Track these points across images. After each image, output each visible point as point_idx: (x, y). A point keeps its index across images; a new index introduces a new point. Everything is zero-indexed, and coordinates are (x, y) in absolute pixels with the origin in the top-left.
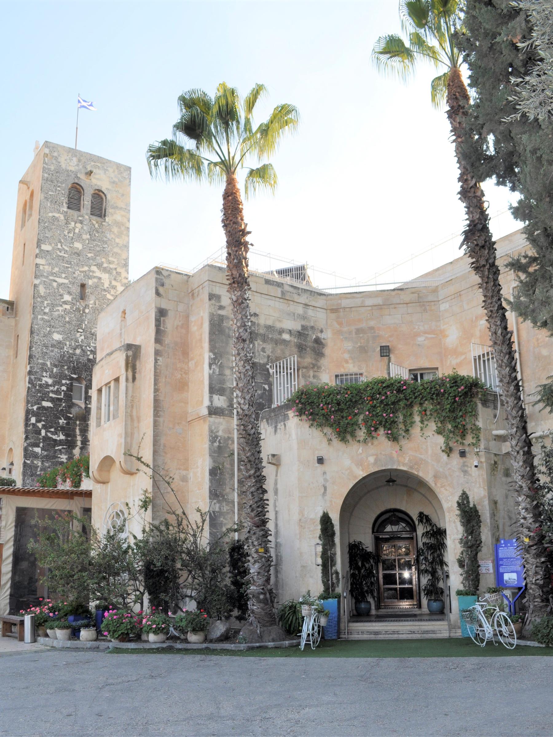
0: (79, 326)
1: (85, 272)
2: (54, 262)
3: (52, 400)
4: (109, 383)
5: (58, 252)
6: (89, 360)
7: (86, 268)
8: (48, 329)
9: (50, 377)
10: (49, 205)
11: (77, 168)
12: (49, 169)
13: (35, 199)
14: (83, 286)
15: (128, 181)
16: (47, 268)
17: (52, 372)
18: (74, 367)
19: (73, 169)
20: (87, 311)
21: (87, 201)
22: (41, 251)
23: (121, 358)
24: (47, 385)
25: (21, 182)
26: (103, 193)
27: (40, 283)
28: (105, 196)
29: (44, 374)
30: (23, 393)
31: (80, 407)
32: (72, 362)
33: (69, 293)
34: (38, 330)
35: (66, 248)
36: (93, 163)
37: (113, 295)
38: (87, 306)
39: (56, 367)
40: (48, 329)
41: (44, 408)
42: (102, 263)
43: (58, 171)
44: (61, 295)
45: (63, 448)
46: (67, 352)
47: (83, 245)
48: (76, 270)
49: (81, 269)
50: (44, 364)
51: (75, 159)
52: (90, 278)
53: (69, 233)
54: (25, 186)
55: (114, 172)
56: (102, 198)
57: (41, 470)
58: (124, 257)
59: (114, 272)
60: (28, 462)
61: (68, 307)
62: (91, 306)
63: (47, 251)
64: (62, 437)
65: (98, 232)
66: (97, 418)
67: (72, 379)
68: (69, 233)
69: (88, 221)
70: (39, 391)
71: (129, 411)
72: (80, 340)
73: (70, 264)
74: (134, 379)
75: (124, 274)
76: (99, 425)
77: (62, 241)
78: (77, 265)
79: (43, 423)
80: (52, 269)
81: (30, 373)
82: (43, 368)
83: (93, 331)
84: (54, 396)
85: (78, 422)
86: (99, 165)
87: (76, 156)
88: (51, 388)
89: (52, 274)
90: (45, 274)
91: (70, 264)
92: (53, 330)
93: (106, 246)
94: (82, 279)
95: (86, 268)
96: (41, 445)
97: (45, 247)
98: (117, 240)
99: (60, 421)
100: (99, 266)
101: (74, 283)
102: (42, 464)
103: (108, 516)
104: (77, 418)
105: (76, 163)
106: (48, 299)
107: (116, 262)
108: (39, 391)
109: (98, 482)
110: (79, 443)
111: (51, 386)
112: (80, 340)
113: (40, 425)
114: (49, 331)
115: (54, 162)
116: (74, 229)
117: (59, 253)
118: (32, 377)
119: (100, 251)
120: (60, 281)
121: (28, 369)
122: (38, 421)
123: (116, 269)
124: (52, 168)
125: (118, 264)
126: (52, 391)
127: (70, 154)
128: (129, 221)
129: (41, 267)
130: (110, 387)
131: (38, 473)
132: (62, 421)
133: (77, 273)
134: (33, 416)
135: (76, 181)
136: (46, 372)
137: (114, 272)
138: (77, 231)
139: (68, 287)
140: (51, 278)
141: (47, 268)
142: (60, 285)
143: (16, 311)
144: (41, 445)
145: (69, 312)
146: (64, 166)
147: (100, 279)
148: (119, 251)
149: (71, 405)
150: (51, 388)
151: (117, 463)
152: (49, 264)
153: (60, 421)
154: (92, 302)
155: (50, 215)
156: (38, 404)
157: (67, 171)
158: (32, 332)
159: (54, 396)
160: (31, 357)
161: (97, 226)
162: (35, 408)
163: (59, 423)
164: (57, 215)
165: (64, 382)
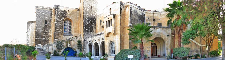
0: (91, 13)
14: (91, 6)
50: (86, 19)
64: (89, 30)
74: (115, 19)
81: (84, 20)
82: (86, 19)
100: (94, 3)
120: (87, 5)
121: (83, 19)
122: (86, 27)
132: (89, 28)
141: (86, 3)
145: (89, 10)
149: (90, 25)
160: (84, 17)
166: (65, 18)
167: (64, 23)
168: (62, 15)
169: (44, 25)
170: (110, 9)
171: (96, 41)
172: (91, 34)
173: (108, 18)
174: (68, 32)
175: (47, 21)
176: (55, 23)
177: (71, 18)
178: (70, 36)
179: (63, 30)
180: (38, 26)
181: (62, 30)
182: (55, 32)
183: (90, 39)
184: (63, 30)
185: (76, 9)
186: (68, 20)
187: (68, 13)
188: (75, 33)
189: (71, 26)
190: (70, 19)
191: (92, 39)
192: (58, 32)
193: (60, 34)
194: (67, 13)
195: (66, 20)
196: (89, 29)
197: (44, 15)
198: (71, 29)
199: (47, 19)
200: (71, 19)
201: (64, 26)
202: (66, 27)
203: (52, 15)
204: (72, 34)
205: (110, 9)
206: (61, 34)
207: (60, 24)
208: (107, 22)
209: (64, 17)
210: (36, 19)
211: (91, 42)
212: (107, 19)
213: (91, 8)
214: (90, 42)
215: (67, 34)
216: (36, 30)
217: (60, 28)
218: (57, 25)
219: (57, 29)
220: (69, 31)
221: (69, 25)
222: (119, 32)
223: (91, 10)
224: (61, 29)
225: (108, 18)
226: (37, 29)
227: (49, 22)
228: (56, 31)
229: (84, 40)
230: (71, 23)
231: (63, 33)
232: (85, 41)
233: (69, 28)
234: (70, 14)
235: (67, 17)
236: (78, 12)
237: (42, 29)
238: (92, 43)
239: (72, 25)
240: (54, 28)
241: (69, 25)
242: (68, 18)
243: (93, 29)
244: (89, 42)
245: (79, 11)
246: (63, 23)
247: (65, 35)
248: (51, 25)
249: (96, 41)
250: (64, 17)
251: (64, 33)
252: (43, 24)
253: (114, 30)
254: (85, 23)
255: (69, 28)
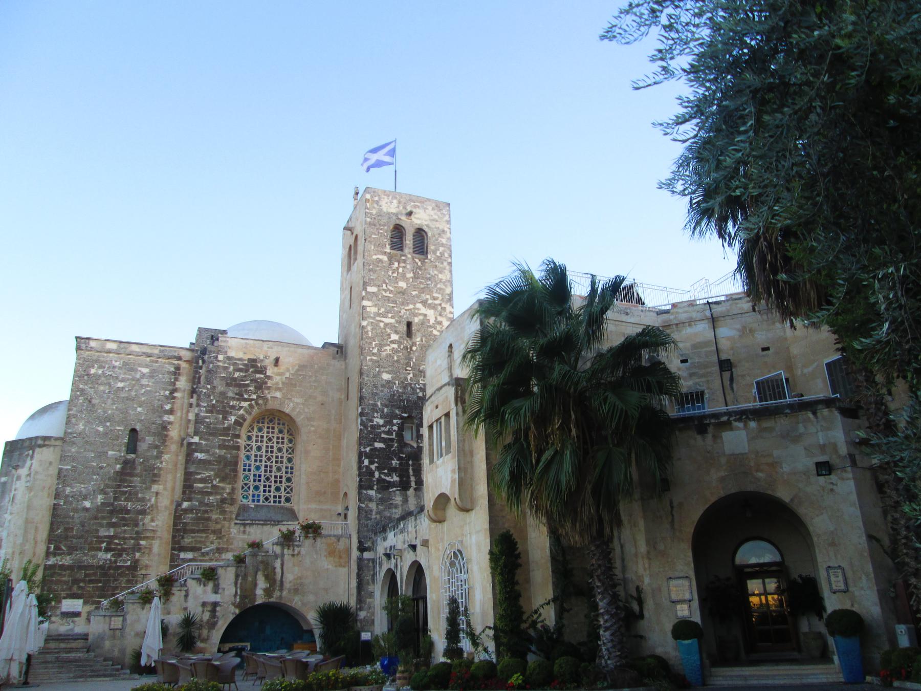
0: (408, 364)
1: (411, 309)
2: (380, 303)
3: (383, 441)
4: (440, 418)
5: (384, 293)
6: (419, 398)
7: (411, 306)
8: (377, 369)
9: (381, 418)
10: (373, 248)
11: (397, 209)
12: (371, 214)
13: (359, 242)
14: (409, 325)
15: (447, 216)
16: (374, 310)
17: (383, 412)
18: (404, 405)
19: (394, 211)
20: (414, 348)
21: (409, 241)
22: (367, 293)
23: (451, 392)
24: (379, 426)
25: (345, 228)
26: (424, 231)
27: (368, 325)
28: (426, 233)
29: (376, 415)
30: (356, 436)
31: (412, 447)
32: (402, 401)
33: (396, 332)
34: (367, 370)
35: (391, 288)
36: (412, 204)
37: (439, 331)
38: (414, 344)
39: (387, 407)
40: (377, 369)
41: (376, 449)
42: (427, 300)
43: (380, 214)
44: (389, 335)
45: (397, 490)
46: (398, 391)
47: (407, 284)
48: (401, 309)
49: (406, 308)
50: (375, 405)
51: (395, 201)
52: (416, 315)
53: (393, 273)
54: (349, 232)
55: (433, 209)
56: (423, 237)
57: (378, 513)
58: (448, 291)
59: (439, 308)
60: (363, 506)
61: (395, 346)
62: (418, 343)
63: (373, 293)
64: (396, 478)
65: (420, 269)
66: (430, 455)
67: (402, 418)
68: (393, 273)
69: (411, 260)
70: (371, 433)
71: (461, 446)
72: (409, 378)
73: (396, 303)
75: (449, 308)
76: (432, 461)
77: (387, 281)
78: (403, 304)
79: (376, 465)
80: (379, 310)
81: (361, 414)
82: (374, 409)
83: (421, 368)
84: (385, 436)
85: (411, 462)
86: (419, 204)
87: (396, 198)
88: (383, 429)
89: (379, 315)
90: (372, 315)
91: (396, 303)
92: (382, 370)
93: (429, 282)
94: (407, 318)
95: (411, 306)
96: (375, 487)
97: (371, 289)
98: (440, 276)
99: (393, 462)
100: (424, 303)
101: (400, 322)
102: (377, 507)
103: (446, 556)
104: (409, 457)
105: (396, 205)
106: (376, 340)
107: (440, 298)
108: (371, 433)
109: (435, 521)
110: (413, 484)
111: (382, 426)
112: (409, 378)
113: (373, 467)
114: (379, 371)
115: (376, 206)
116: (398, 269)
117: (384, 294)
118: (364, 418)
119: (424, 288)
120: (387, 320)
122: (371, 463)
123: (440, 305)
124: (374, 212)
125: (442, 300)
126: (384, 432)
127: (390, 198)
128: (450, 256)
129: (368, 309)
130: (440, 423)
131: (373, 517)
132: (395, 462)
133: (403, 311)
134: (366, 458)
135: (398, 222)
136: (377, 412)
137: (439, 308)
138: (401, 270)
139: (395, 326)
140: (378, 318)
141: (374, 310)
142: (386, 325)
143: (346, 354)
144: (375, 487)
146: (385, 210)
147: (425, 315)
148: (443, 287)
149: (403, 444)
150: (383, 429)
151: (453, 500)
152: (375, 305)
153: (393, 462)
154: (419, 339)
155: (375, 257)
156: (371, 445)
157: (388, 213)
158: (361, 374)
159: (385, 436)
160: (361, 398)
161: (419, 264)
162: (368, 449)
163: (392, 464)
164: (381, 257)
165: (395, 421)
166: (256, 410)
167: (249, 438)
168: (236, 390)
169: (117, 460)
170: (451, 346)
171: (413, 547)
172: (405, 501)
173: (437, 407)
174: (267, 499)
175: (141, 435)
176: (190, 444)
177: (294, 409)
178: (278, 522)
179: (240, 483)
180: (74, 469)
181: (228, 488)
182: (185, 505)
183: (393, 539)
184: (233, 489)
185: (326, 345)
186: (271, 421)
187: (277, 379)
188: (313, 506)
189: (290, 460)
190: (287, 411)
191: (400, 537)
192: (202, 503)
193: (214, 516)
194: (269, 378)
195: (260, 419)
196: (392, 470)
197: (123, 395)
198: (289, 480)
199: (140, 421)
200: (293, 415)
201: (248, 458)
202: (258, 468)
203: (172, 392)
204: (295, 508)
205: (451, 346)
206: (223, 512)
207: (221, 447)
208: (431, 427)
209: (245, 404)
210: (68, 422)
211: (393, 561)
212: (432, 411)
213: (409, 333)
214: (388, 556)
215: (263, 514)
216: (57, 496)
217: (216, 476)
218: (200, 456)
219: (203, 481)
220: (278, 489)
221: (280, 450)
222: (482, 489)
223: (408, 350)
224: (223, 480)
225: (437, 407)
226: (68, 490)
227: (149, 440)
228: (189, 500)
229: (362, 549)
230: (290, 441)
231: (234, 509)
232: (367, 555)
233: (279, 469)
234: (290, 384)
235: (266, 400)
236: (338, 364)
237: (103, 492)
238: (396, 566)
239: (299, 448)
240: (180, 475)
241: (280, 450)
242: (271, 405)
243: (418, 472)
244: (384, 558)
245: (345, 359)
246: (242, 442)
247: (245, 517)
248: (166, 457)
249: (413, 547)
250: (245, 400)
251: (244, 508)
252: (110, 453)
253: (457, 476)
254: (368, 434)
255: (279, 469)
